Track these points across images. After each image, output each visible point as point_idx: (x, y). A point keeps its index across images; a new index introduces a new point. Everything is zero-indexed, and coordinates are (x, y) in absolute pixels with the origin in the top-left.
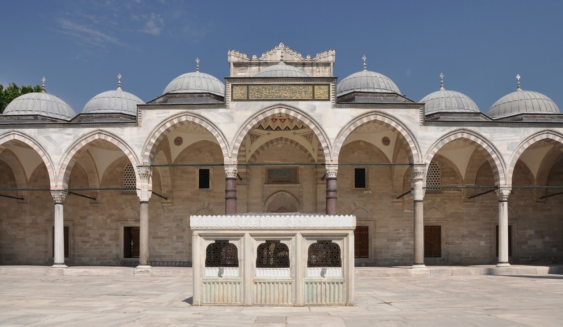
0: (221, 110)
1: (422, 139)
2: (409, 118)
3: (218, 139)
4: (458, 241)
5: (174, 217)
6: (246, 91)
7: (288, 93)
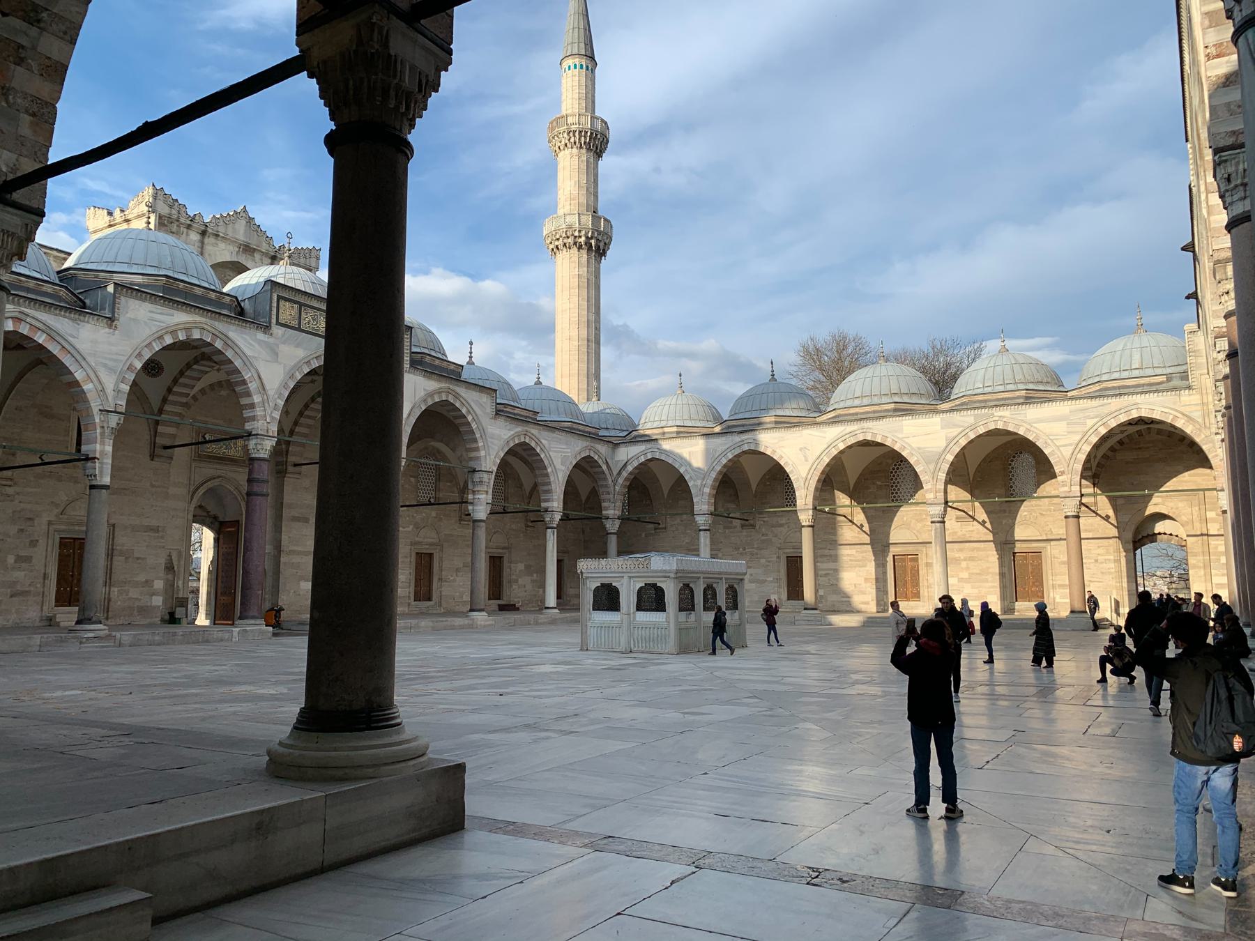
0: (261, 336)
1: (492, 438)
2: (481, 405)
4: (452, 576)
5: (14, 512)
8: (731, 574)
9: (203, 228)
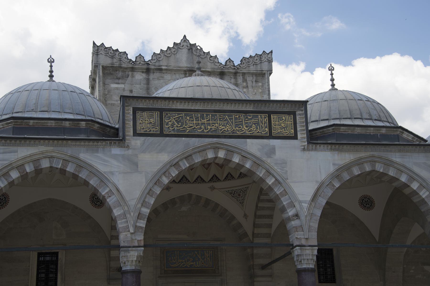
0: (116, 151)
3: (110, 201)
6: (158, 120)
7: (228, 125)
9: (145, 67)
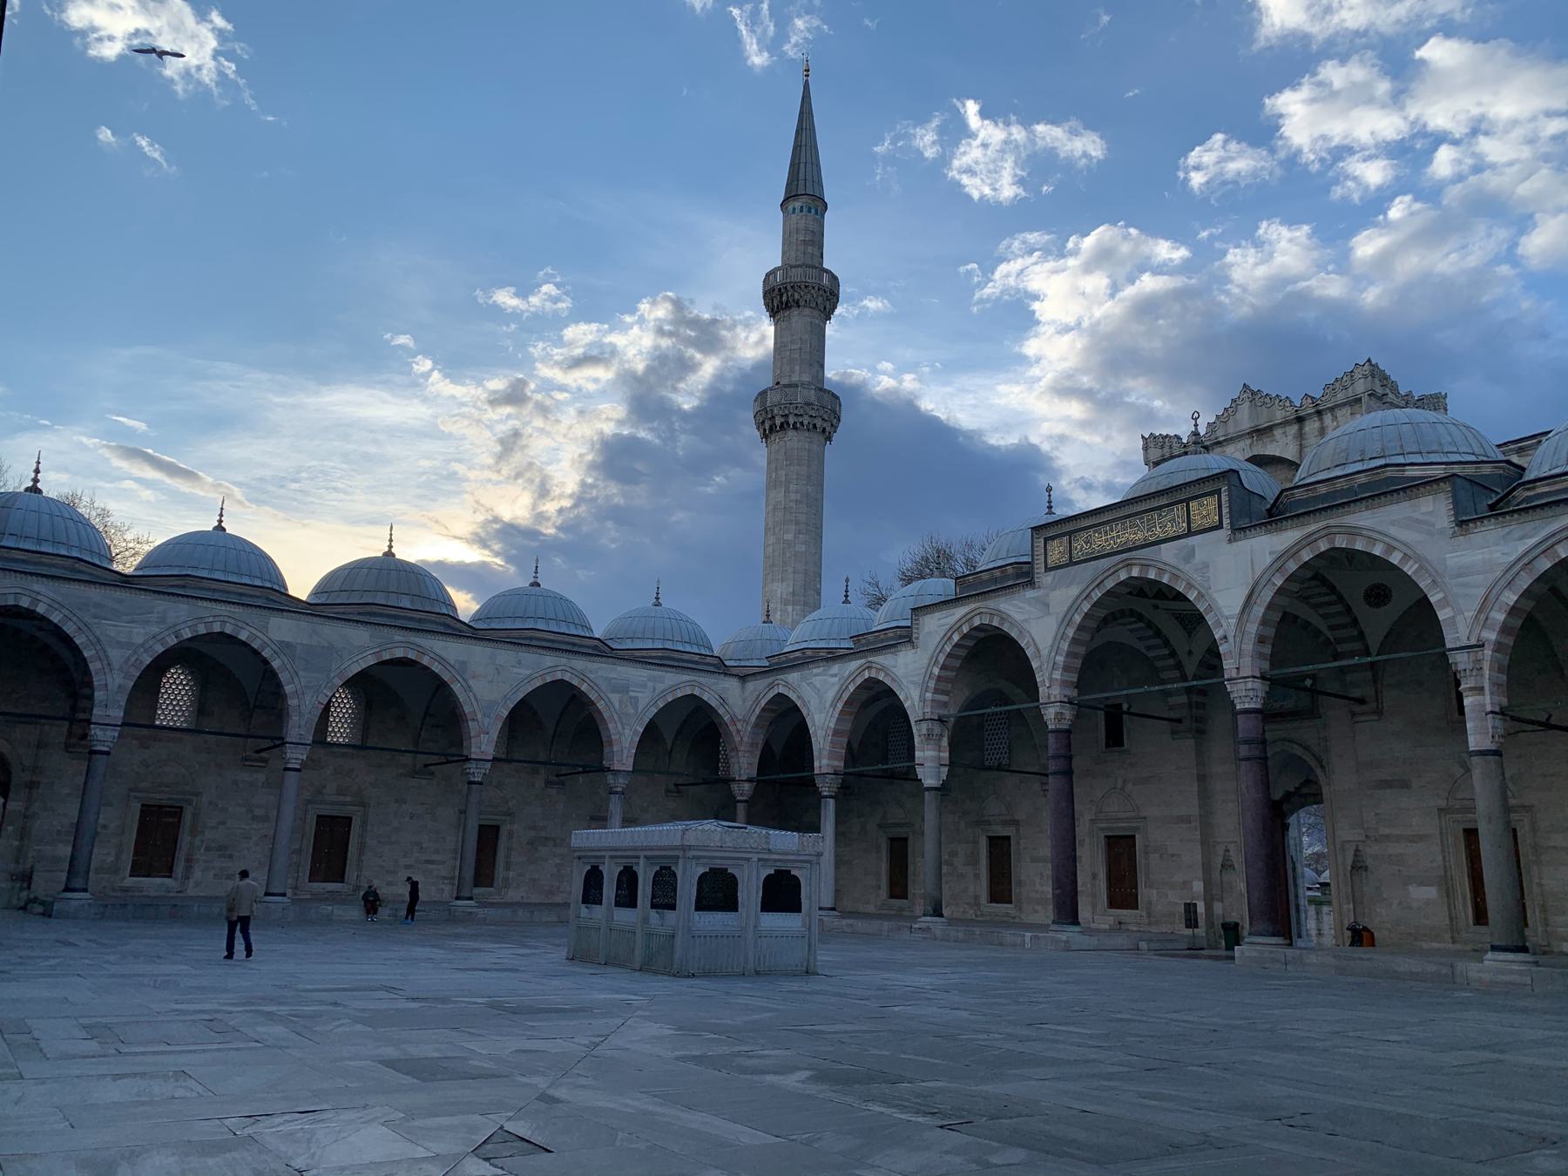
8: (651, 849)
